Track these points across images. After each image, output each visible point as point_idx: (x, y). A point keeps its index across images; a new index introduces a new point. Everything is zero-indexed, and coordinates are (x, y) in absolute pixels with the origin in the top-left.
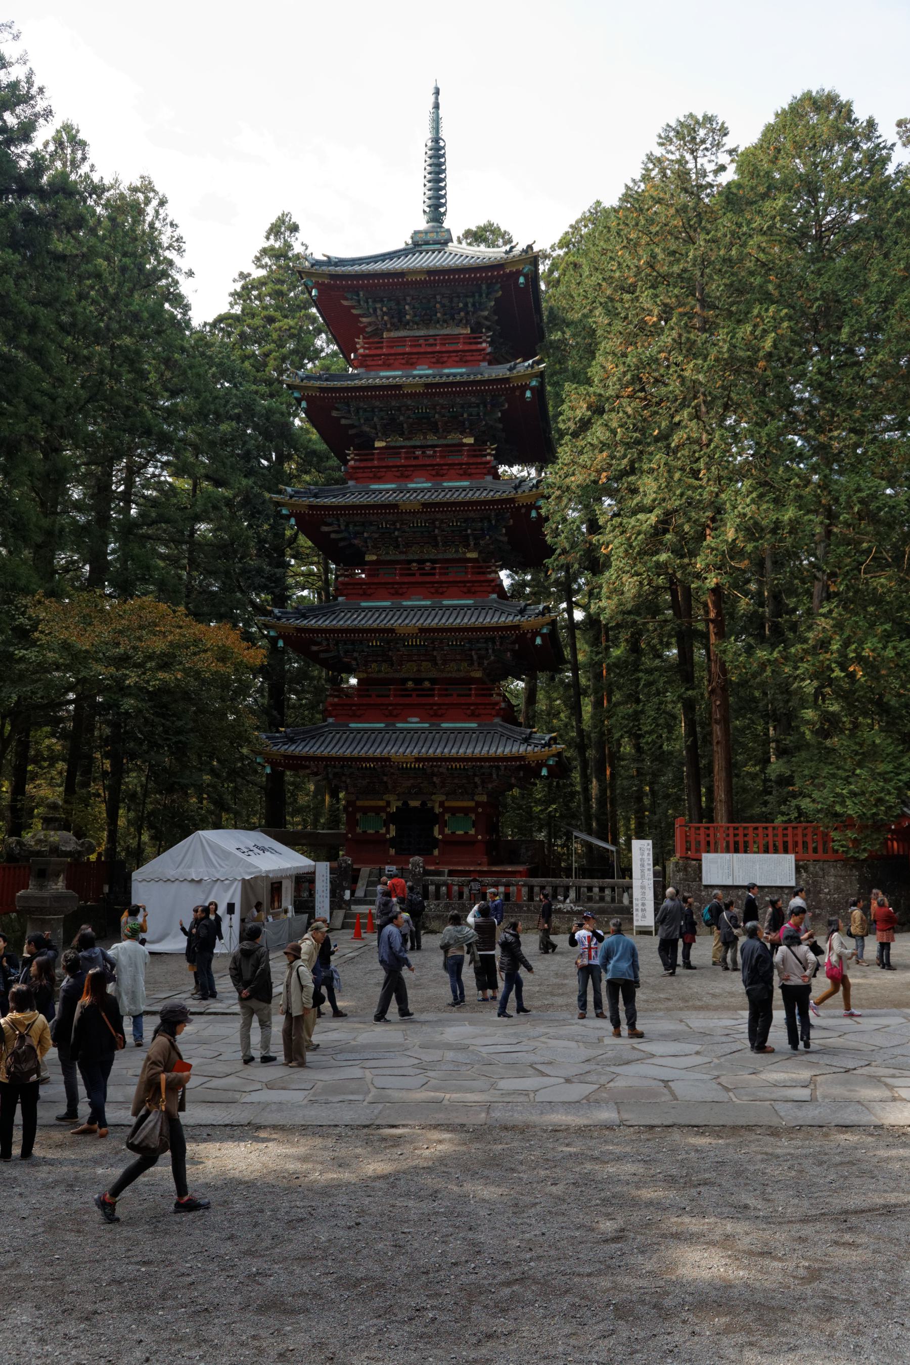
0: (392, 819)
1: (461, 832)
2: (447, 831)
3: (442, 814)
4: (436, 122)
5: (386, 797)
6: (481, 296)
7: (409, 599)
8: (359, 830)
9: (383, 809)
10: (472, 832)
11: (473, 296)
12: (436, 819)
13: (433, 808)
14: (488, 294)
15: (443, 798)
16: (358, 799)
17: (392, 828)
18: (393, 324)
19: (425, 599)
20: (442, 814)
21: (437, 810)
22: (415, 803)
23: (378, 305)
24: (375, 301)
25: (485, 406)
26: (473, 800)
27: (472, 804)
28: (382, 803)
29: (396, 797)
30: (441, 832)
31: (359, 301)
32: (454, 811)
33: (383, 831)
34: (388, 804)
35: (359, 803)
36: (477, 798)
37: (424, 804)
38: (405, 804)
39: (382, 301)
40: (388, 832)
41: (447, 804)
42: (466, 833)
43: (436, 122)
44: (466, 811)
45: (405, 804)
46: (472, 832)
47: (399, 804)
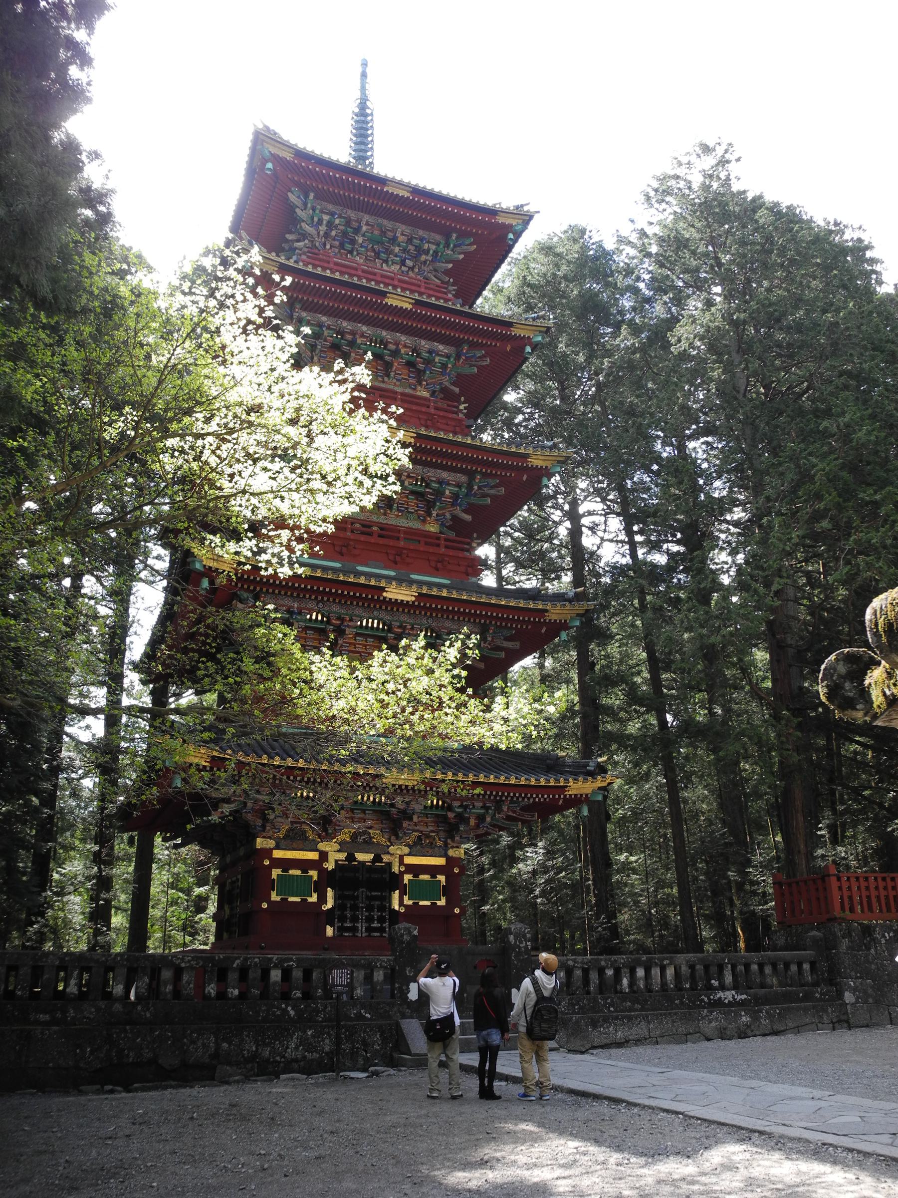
0: (328, 879)
1: (427, 903)
2: (407, 901)
3: (402, 874)
4: (363, 89)
5: (322, 846)
6: (447, 245)
7: (366, 565)
8: (275, 897)
9: (316, 865)
10: (442, 902)
11: (438, 244)
12: (395, 882)
13: (389, 865)
14: (455, 246)
15: (406, 850)
16: (277, 847)
17: (330, 893)
18: (331, 247)
19: (386, 568)
20: (402, 874)
21: (396, 869)
22: (364, 857)
23: (326, 218)
24: (322, 212)
25: (458, 357)
26: (445, 855)
27: (440, 861)
28: (313, 856)
29: (337, 847)
30: (401, 903)
31: (305, 205)
32: (415, 870)
33: (314, 899)
34: (324, 856)
35: (278, 854)
36: (451, 853)
37: (378, 858)
38: (351, 858)
39: (332, 214)
40: (323, 899)
41: (409, 860)
42: (434, 904)
43: (363, 89)
44: (433, 870)
45: (351, 858)
46: (442, 902)
47: (342, 856)
